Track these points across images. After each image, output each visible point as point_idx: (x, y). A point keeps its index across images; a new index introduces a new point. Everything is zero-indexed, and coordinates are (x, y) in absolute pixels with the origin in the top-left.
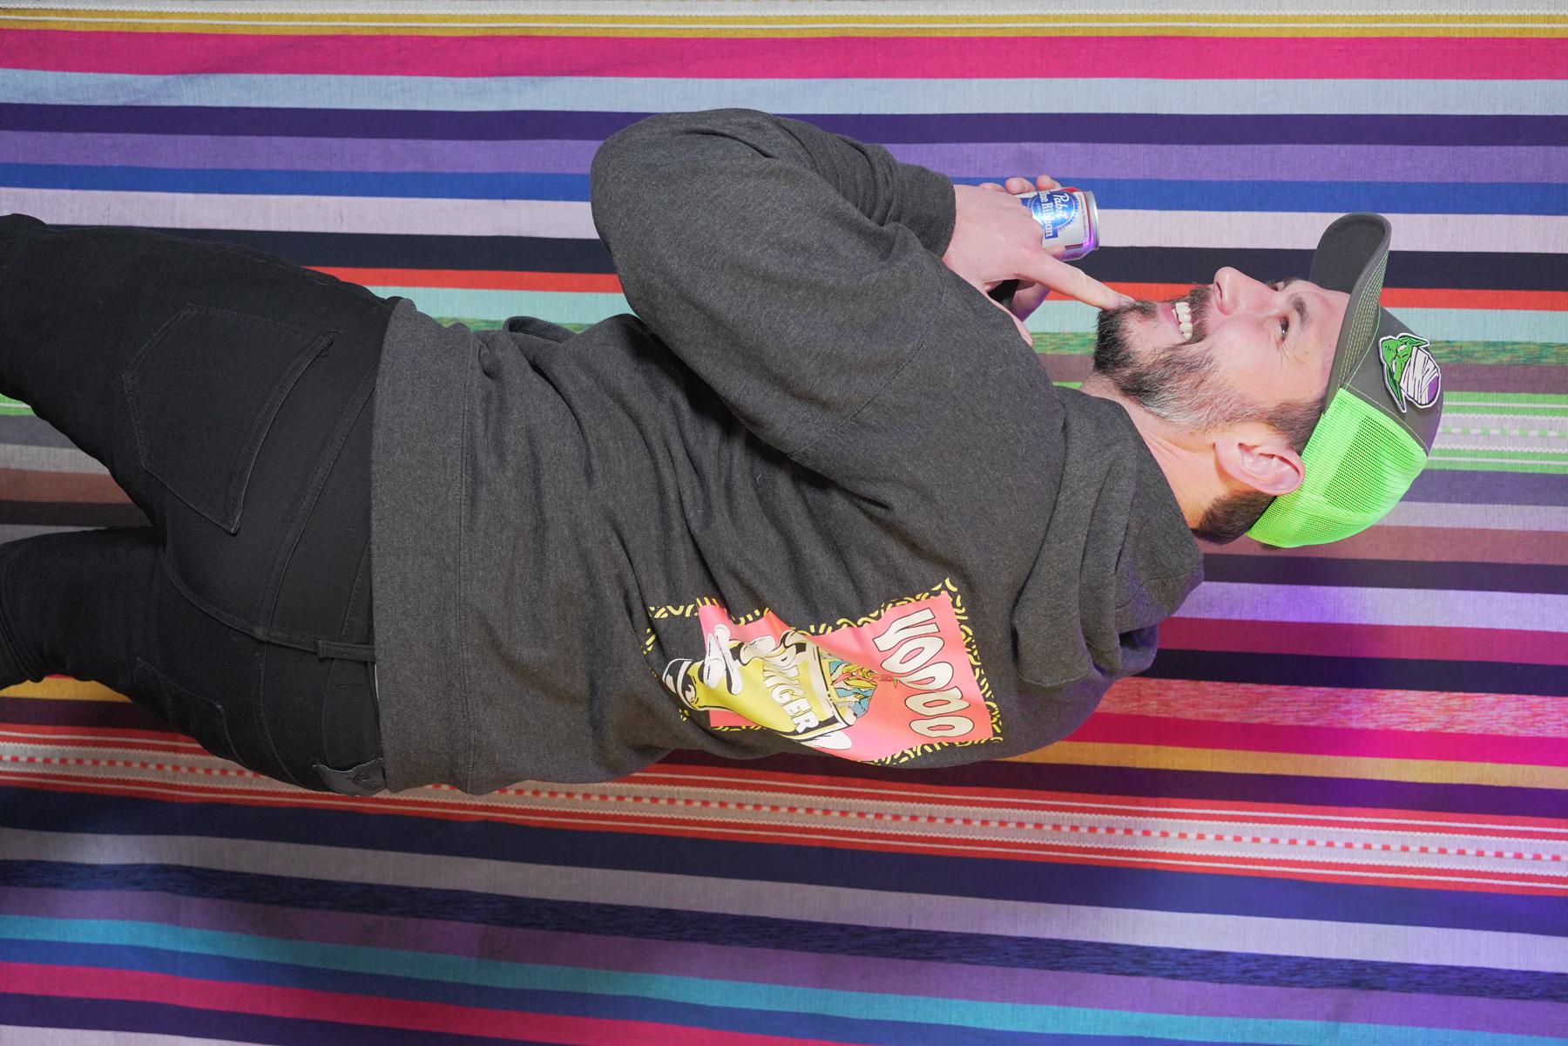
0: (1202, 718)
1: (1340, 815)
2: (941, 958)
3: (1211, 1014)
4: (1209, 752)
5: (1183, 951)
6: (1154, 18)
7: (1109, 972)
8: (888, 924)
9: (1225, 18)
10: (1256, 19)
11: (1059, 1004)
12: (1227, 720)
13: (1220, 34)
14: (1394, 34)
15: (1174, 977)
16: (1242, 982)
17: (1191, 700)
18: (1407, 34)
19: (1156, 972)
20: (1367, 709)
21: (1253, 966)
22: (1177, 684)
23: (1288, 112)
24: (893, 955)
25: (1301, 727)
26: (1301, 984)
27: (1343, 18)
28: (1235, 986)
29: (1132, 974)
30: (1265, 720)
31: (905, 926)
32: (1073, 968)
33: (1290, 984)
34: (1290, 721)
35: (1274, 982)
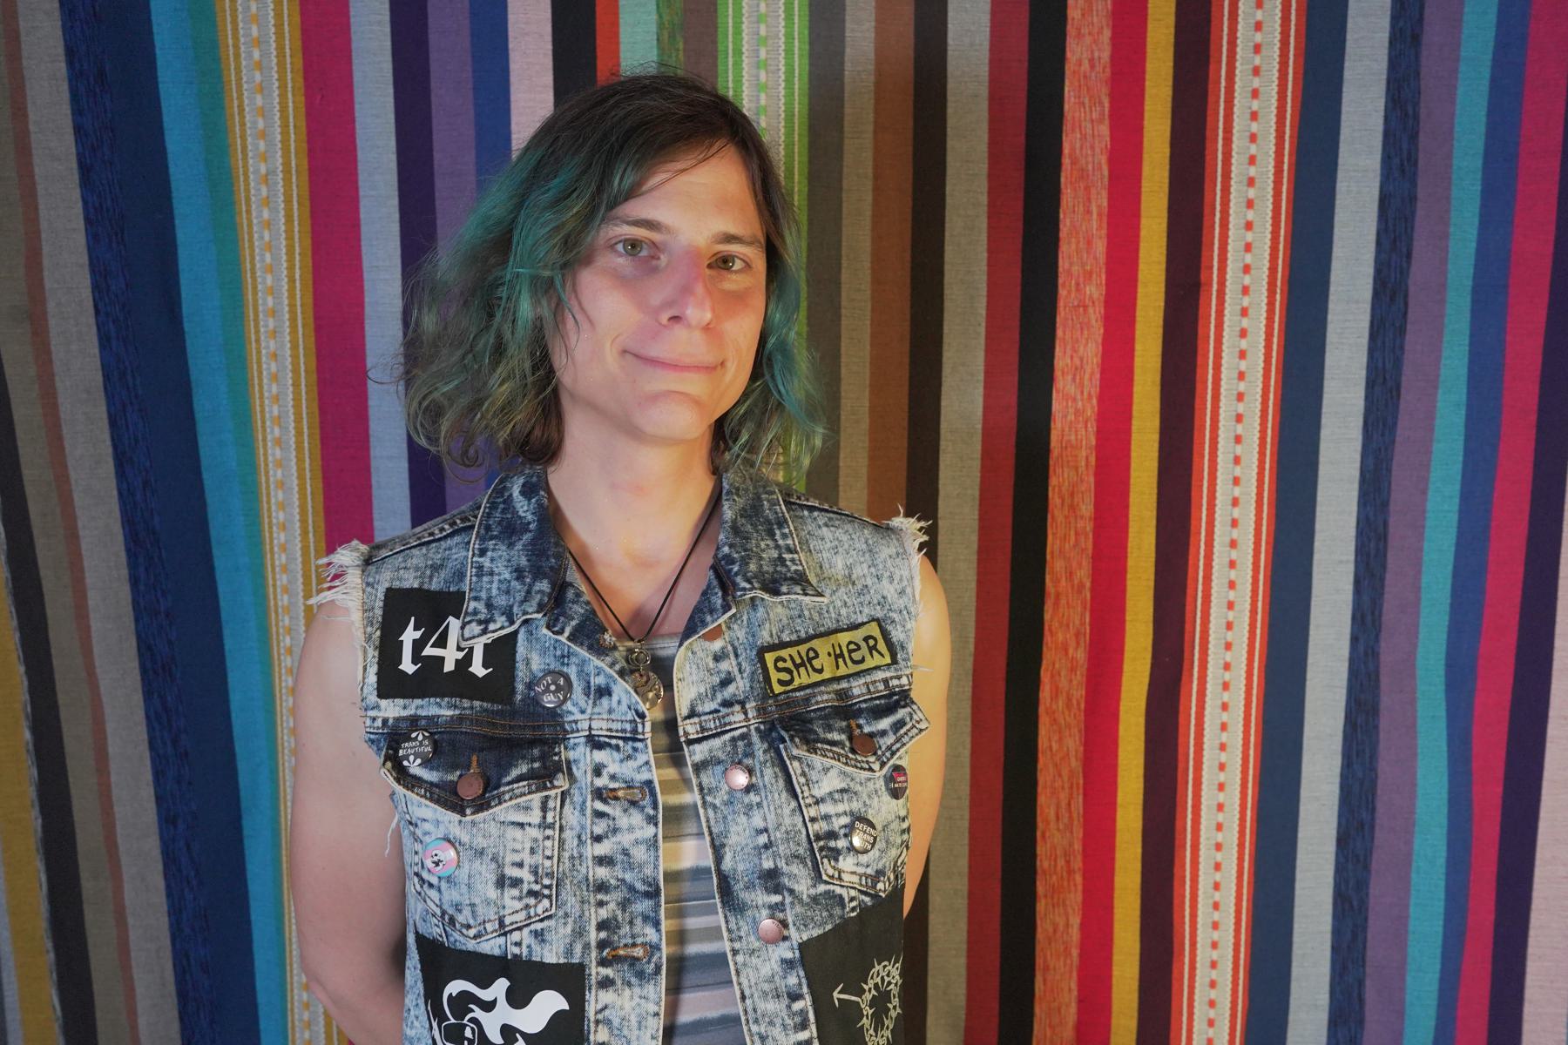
0: (1104, 232)
1: (1220, 62)
2: (1386, 524)
3: (1448, 211)
4: (1144, 222)
5: (1379, 243)
6: (293, 320)
7: (1401, 331)
8: (1348, 587)
9: (290, 238)
10: (288, 201)
11: (1436, 388)
12: (1105, 203)
13: (308, 242)
14: (298, 34)
15: (1409, 255)
16: (1415, 174)
17: (1081, 245)
18: (297, 19)
19: (1404, 273)
20: (1088, 40)
21: (1396, 161)
22: (1063, 264)
23: (394, 157)
24: (1382, 580)
25: (1111, 116)
26: (1416, 105)
27: (283, 96)
28: (1420, 182)
29: (1406, 304)
30: (1104, 160)
31: (1351, 567)
32: (1399, 375)
33: (1416, 117)
34: (1105, 129)
35: (1414, 137)
